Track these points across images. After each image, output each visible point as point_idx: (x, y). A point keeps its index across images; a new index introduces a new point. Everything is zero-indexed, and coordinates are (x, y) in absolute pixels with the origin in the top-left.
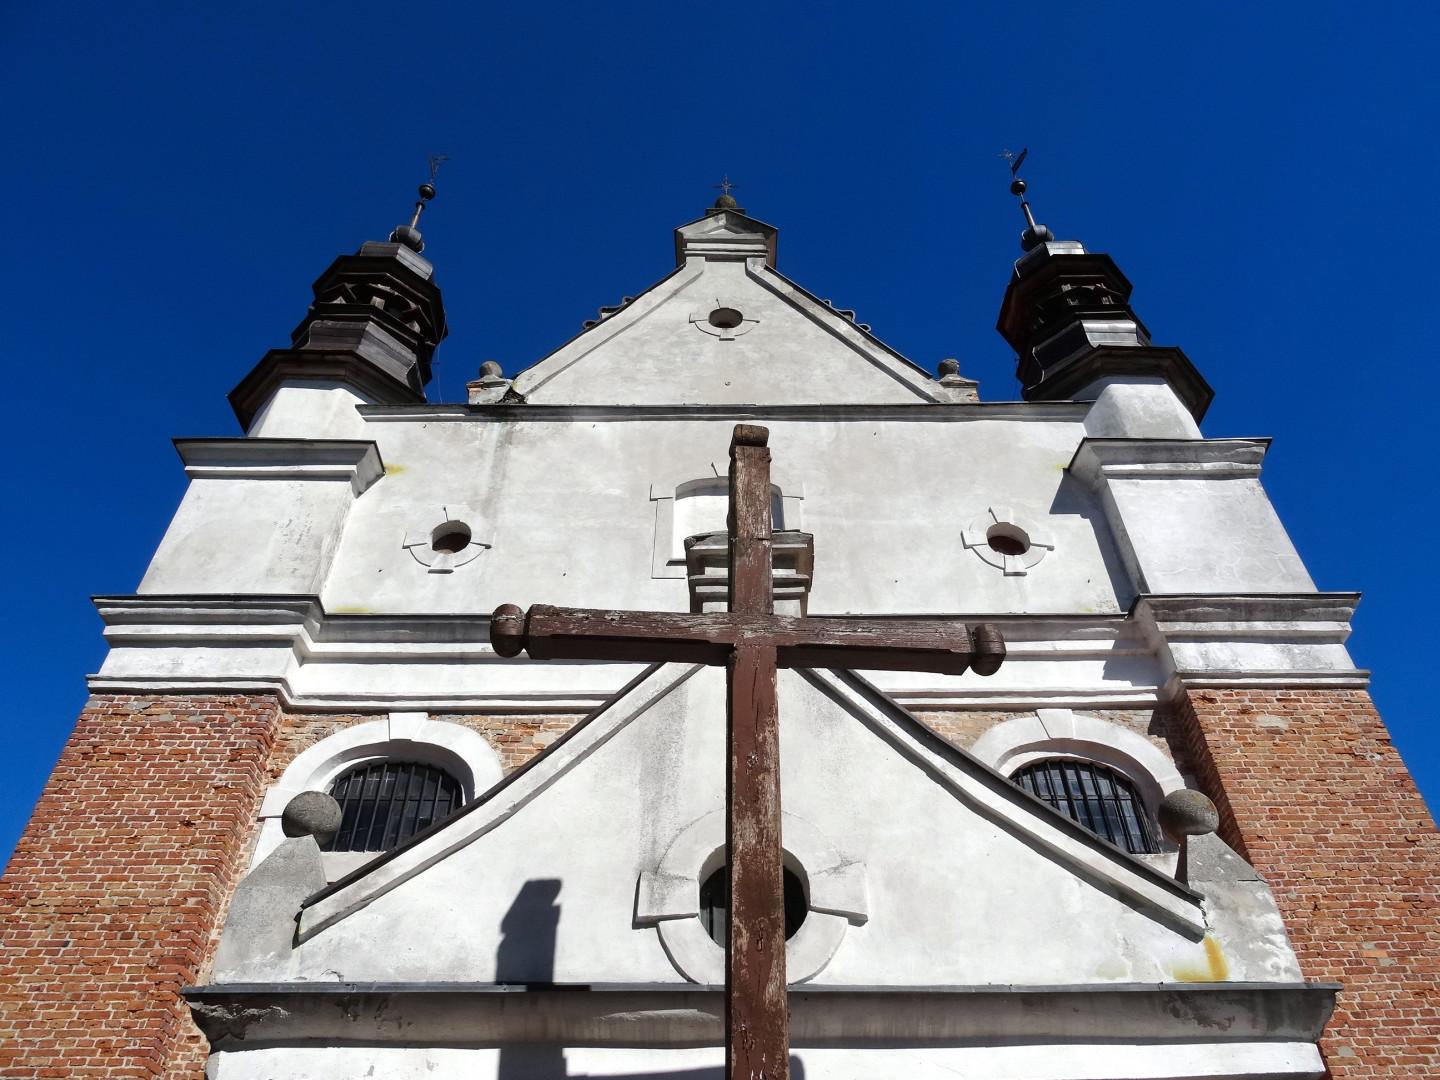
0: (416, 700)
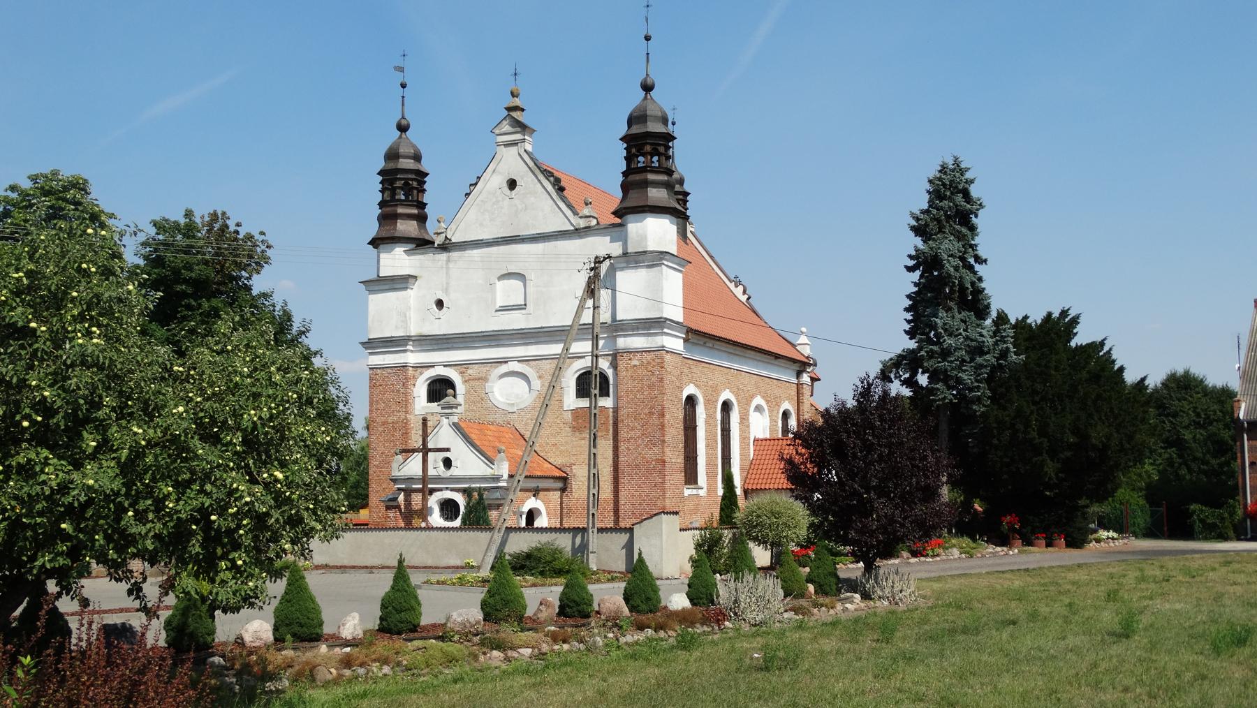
0: (440, 362)
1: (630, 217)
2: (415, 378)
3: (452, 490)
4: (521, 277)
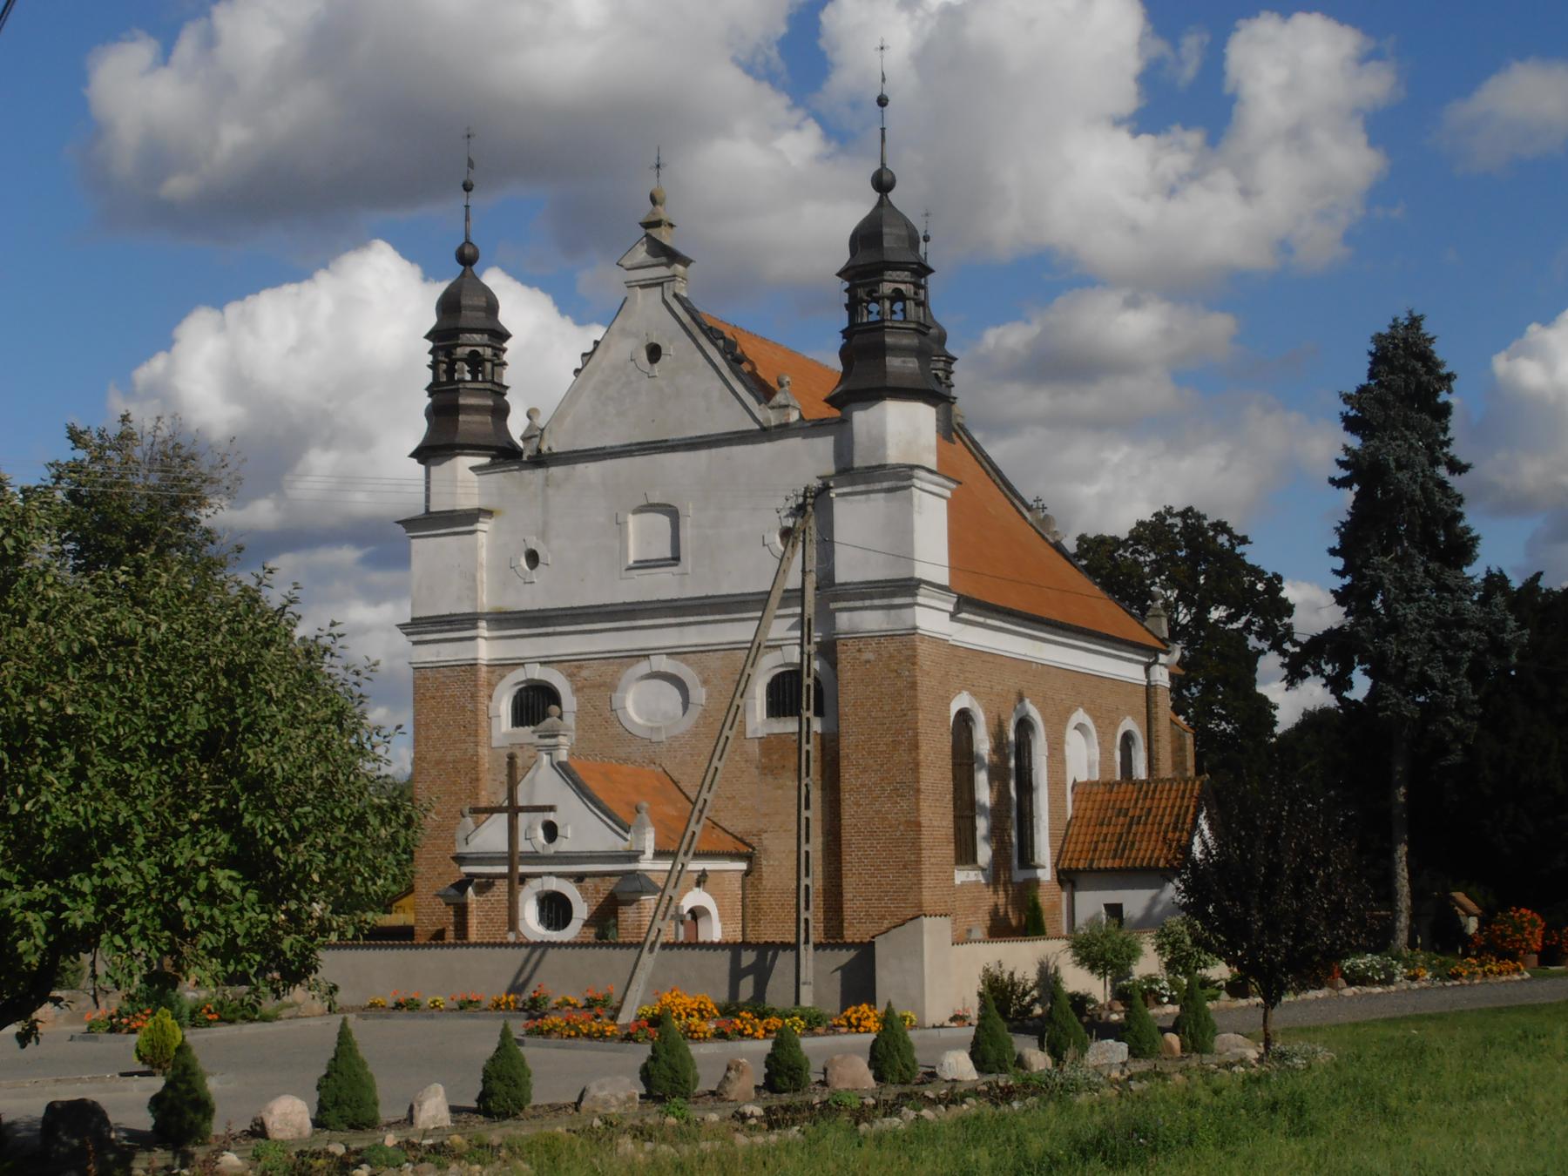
0: (537, 655)
1: (853, 405)
2: (491, 685)
3: (559, 875)
4: (673, 513)
